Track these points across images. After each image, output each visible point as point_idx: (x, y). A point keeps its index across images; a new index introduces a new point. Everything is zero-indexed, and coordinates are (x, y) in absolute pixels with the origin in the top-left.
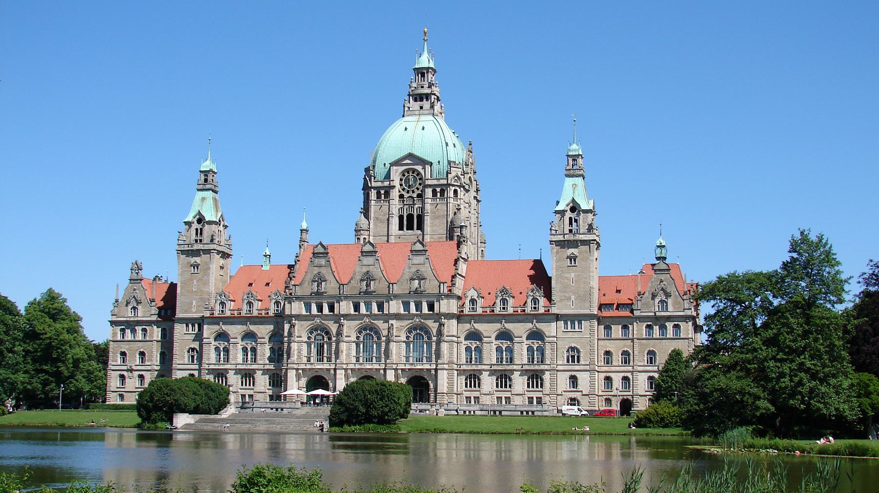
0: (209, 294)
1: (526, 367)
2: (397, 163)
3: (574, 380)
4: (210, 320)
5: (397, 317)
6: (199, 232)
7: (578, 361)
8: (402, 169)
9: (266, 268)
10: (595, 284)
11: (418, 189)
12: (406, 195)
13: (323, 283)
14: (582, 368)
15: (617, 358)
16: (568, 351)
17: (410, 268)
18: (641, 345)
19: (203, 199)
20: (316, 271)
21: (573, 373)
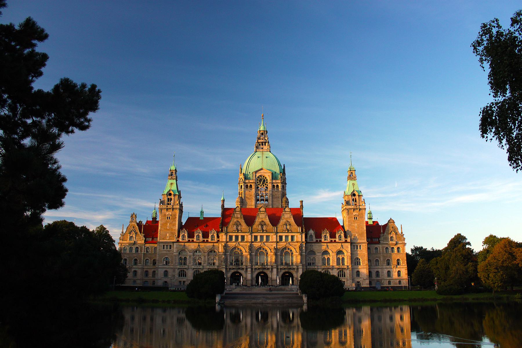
0: (175, 230)
1: (338, 267)
2: (256, 172)
8: (258, 175)
9: (202, 219)
10: (365, 228)
14: (362, 267)
18: (384, 256)
19: (172, 184)
20: (235, 220)
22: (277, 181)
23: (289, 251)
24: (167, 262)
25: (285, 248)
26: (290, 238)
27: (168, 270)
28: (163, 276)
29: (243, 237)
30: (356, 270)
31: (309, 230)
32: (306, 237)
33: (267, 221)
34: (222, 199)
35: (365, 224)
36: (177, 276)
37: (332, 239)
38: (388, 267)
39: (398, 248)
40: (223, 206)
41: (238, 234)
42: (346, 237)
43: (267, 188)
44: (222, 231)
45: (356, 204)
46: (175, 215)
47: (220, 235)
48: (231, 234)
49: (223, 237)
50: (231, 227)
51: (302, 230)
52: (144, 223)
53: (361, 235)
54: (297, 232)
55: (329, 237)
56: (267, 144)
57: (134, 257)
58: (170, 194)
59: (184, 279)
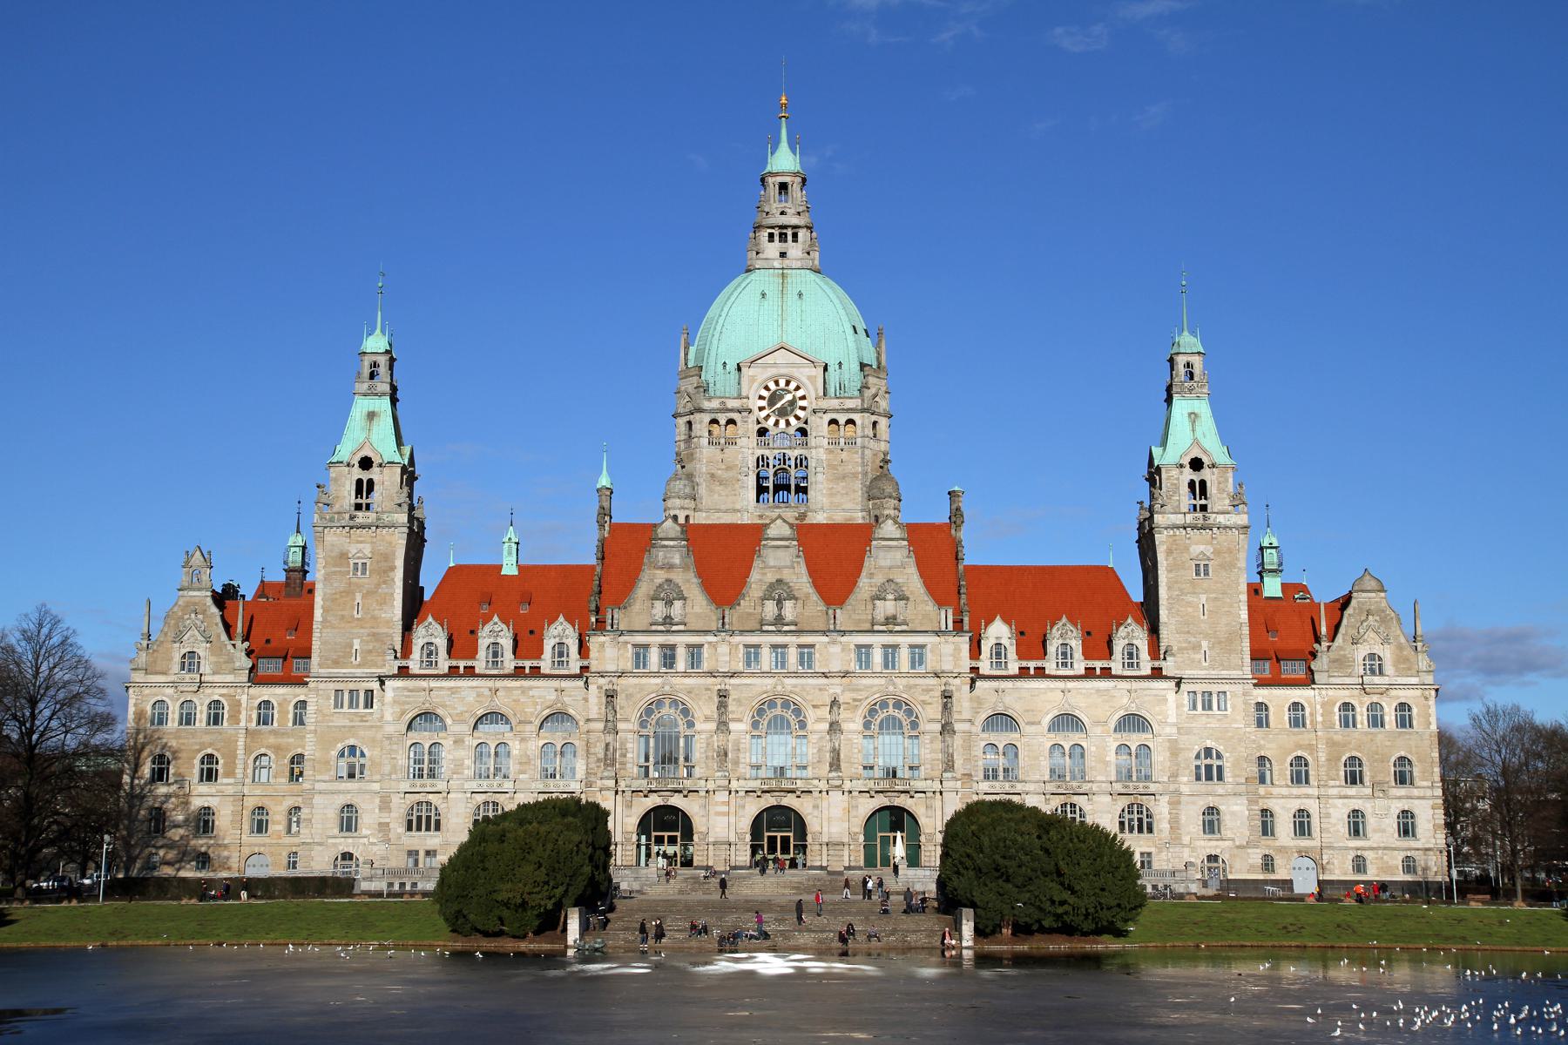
0: (389, 623)
3: (1211, 820)
4: (399, 683)
5: (845, 674)
6: (364, 488)
7: (1220, 778)
9: (510, 569)
10: (1244, 615)
11: (797, 418)
12: (773, 431)
13: (678, 604)
15: (1281, 771)
16: (1198, 757)
17: (871, 575)
18: (1332, 744)
19: (371, 416)
20: (661, 576)
21: (1211, 801)
22: (850, 404)
23: (900, 714)
24: (351, 767)
25: (884, 705)
26: (904, 655)
27: (355, 801)
28: (336, 831)
29: (695, 651)
30: (1203, 803)
31: (989, 622)
32: (975, 651)
33: (800, 580)
34: (604, 481)
35: (1244, 597)
36: (399, 828)
37: (1091, 664)
38: (1352, 791)
39: (1403, 706)
40: (604, 513)
41: (671, 639)
42: (1155, 651)
43: (803, 432)
44: (600, 626)
45: (1204, 508)
46: (388, 557)
47: (595, 642)
48: (640, 639)
49: (608, 653)
50: (641, 609)
51: (958, 624)
52: (248, 590)
53: (1225, 644)
54: (937, 633)
55: (1078, 654)
56: (802, 234)
57: (203, 746)
58: (366, 463)
59: (430, 840)
